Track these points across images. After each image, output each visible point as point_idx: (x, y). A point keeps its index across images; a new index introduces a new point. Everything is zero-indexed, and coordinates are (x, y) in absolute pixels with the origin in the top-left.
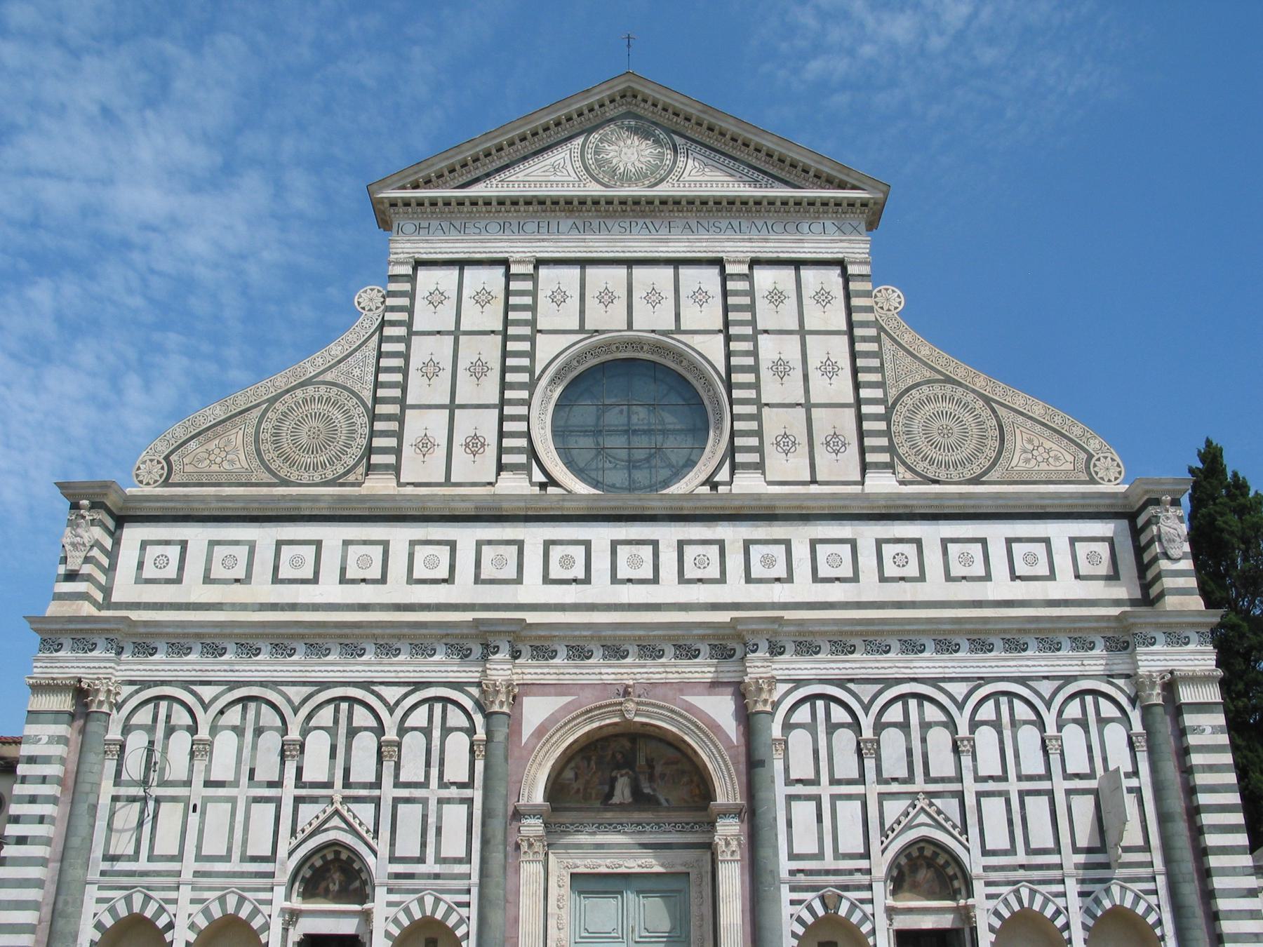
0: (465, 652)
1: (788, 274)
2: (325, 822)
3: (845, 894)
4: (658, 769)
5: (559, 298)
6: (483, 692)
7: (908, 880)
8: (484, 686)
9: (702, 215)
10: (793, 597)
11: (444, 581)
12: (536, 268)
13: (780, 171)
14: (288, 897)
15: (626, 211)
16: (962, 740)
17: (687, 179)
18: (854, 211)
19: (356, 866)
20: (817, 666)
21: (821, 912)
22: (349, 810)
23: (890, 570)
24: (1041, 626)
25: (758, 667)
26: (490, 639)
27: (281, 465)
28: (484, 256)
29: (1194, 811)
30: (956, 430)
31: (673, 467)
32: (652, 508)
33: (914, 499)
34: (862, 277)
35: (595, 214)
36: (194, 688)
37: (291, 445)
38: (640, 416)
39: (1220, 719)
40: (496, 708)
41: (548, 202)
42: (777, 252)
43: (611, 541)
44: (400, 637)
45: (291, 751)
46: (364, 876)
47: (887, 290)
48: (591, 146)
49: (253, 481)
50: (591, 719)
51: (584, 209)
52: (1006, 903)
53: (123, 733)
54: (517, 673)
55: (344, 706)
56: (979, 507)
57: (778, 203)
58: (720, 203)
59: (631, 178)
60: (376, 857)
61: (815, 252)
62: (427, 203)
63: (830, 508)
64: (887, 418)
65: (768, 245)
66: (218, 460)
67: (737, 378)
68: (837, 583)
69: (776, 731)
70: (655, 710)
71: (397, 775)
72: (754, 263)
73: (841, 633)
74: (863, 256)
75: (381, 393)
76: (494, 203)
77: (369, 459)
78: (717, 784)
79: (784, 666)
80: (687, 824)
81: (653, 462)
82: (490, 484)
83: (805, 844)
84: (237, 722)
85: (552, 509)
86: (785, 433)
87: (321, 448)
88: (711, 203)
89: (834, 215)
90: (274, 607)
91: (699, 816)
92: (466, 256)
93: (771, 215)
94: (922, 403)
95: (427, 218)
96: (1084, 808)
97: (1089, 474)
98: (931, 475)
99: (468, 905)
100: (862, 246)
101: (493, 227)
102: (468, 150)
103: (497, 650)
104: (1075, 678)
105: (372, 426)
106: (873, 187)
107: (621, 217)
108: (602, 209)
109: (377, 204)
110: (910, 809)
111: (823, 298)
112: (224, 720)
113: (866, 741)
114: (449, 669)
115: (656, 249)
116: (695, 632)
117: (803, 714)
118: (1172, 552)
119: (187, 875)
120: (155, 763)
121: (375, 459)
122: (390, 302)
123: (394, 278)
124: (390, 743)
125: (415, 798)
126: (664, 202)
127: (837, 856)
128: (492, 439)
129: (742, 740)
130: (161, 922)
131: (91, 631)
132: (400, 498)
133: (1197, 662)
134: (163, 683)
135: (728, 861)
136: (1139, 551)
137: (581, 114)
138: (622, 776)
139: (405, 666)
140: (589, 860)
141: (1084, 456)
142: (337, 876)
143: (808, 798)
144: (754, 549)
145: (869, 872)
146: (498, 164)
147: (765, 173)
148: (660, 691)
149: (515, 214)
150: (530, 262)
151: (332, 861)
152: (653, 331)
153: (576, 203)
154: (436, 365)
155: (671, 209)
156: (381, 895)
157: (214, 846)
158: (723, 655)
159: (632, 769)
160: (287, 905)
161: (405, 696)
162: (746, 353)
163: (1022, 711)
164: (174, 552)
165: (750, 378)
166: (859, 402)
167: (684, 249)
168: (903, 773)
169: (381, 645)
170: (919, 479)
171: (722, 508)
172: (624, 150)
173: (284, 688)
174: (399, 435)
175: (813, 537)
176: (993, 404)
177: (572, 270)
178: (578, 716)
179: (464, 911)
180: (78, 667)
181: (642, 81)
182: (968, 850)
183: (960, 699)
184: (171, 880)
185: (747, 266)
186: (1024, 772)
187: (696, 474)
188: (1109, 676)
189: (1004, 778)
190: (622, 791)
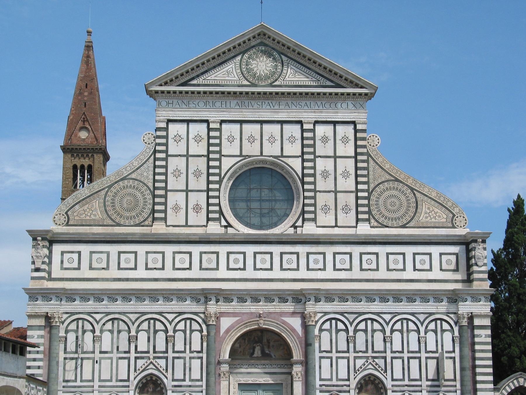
0: (198, 300)
1: (331, 127)
2: (147, 366)
5: (231, 139)
6: (205, 316)
7: (364, 389)
8: (206, 314)
11: (188, 269)
12: (221, 124)
13: (329, 76)
15: (260, 97)
16: (387, 337)
17: (288, 79)
18: (361, 97)
19: (159, 382)
20: (333, 307)
22: (156, 362)
23: (365, 266)
24: (422, 293)
25: (310, 307)
26: (208, 295)
27: (116, 217)
28: (198, 118)
29: (474, 367)
31: (279, 216)
32: (270, 239)
35: (246, 98)
36: (92, 315)
38: (265, 193)
39: (489, 332)
40: (211, 323)
42: (326, 118)
43: (254, 252)
44: (172, 294)
45: (132, 339)
46: (162, 386)
49: (105, 224)
50: (247, 327)
53: (65, 333)
54: (218, 308)
55: (152, 321)
56: (403, 239)
57: (328, 94)
60: (167, 379)
63: (342, 239)
64: (368, 198)
65: (322, 114)
66: (89, 214)
68: (343, 271)
69: (316, 332)
70: (271, 323)
71: (173, 348)
73: (343, 294)
78: (293, 352)
79: (320, 307)
80: (282, 365)
81: (271, 214)
83: (326, 375)
84: (110, 328)
85: (230, 238)
89: (352, 99)
90: (119, 280)
91: (287, 362)
94: (384, 191)
95: (170, 99)
96: (432, 364)
97: (453, 224)
98: (385, 224)
100: (364, 115)
103: (210, 300)
104: (434, 314)
107: (258, 100)
110: (366, 363)
111: (345, 140)
112: (105, 328)
113: (350, 337)
114: (192, 307)
115: (273, 116)
116: (287, 293)
117: (327, 326)
118: (479, 263)
119: (96, 387)
120: (80, 345)
121: (157, 215)
122: (158, 141)
124: (171, 336)
125: (181, 357)
127: (338, 380)
129: (304, 335)
131: (49, 293)
133: (482, 309)
134: (80, 313)
135: (297, 381)
136: (469, 259)
138: (257, 346)
139: (175, 306)
140: (245, 378)
141: (451, 215)
142: (151, 386)
143: (327, 358)
144: (311, 256)
145: (349, 386)
146: (202, 70)
147: (323, 76)
148: (273, 315)
149: (211, 98)
151: (149, 380)
152: (271, 156)
154: (179, 171)
155: (280, 96)
157: (106, 375)
158: (297, 301)
159: (261, 343)
161: (176, 317)
163: (412, 326)
164: (75, 256)
165: (311, 179)
166: (357, 191)
167: (285, 116)
168: (364, 349)
169: (165, 297)
170: (380, 225)
171: (299, 239)
172: (260, 63)
173: (128, 315)
174: (165, 204)
177: (236, 126)
178: (242, 325)
180: (46, 308)
182: (387, 379)
183: (387, 321)
184: (90, 389)
185: (313, 125)
186: (410, 350)
188: (447, 313)
189: (402, 352)
190: (258, 352)
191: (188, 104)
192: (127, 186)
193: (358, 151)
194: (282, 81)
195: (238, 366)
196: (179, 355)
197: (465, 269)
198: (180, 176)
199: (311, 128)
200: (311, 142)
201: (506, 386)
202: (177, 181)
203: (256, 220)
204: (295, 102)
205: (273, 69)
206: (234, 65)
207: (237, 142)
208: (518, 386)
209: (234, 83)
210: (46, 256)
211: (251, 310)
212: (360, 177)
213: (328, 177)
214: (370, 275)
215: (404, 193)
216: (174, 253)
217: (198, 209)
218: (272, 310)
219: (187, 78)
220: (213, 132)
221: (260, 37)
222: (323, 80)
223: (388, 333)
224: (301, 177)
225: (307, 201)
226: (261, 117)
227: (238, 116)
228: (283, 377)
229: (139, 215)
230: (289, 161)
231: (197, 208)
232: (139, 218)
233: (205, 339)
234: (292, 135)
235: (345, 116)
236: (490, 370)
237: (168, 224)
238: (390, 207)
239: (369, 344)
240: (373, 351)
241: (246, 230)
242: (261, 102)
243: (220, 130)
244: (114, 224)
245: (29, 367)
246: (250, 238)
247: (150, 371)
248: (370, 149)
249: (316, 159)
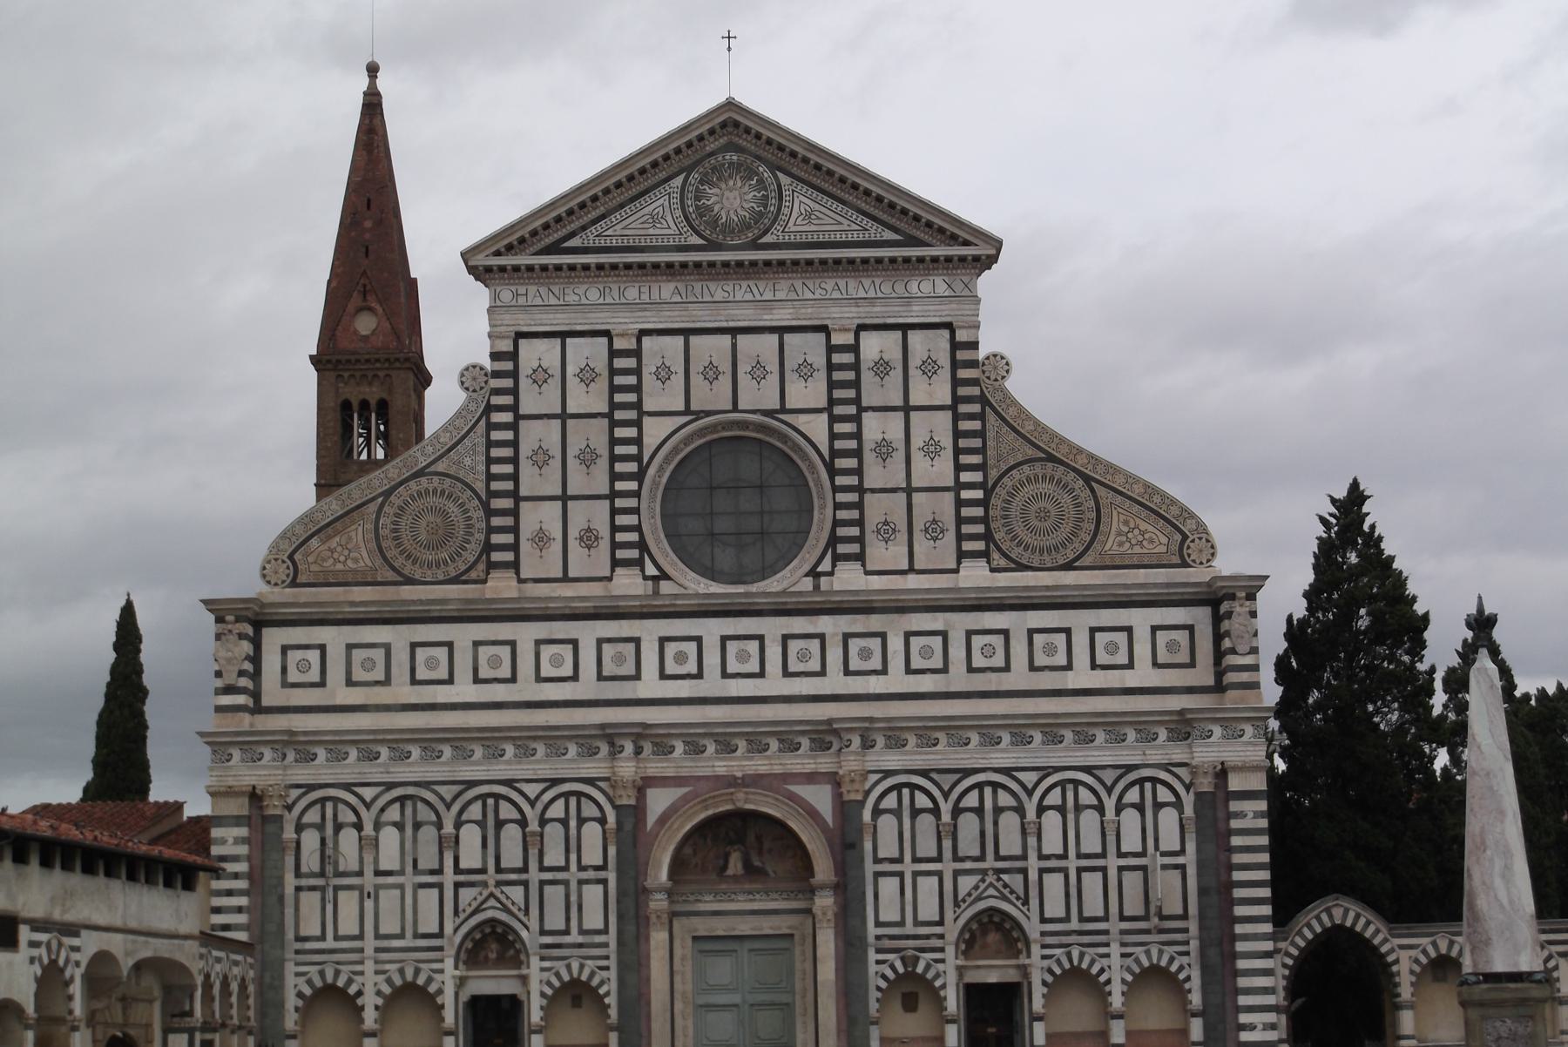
2: (482, 903)
3: (922, 955)
4: (767, 845)
5: (663, 374)
10: (887, 689)
12: (639, 341)
14: (456, 968)
16: (1029, 823)
19: (510, 938)
21: (901, 970)
22: (502, 892)
23: (978, 661)
30: (1053, 513)
35: (697, 277)
37: (411, 542)
39: (1263, 805)
40: (625, 801)
44: (535, 738)
46: (518, 946)
48: (691, 189)
49: (379, 579)
50: (706, 808)
51: (686, 272)
52: (1059, 962)
53: (296, 833)
61: (923, 316)
66: (342, 558)
69: (867, 815)
71: (541, 861)
72: (862, 328)
83: (889, 913)
87: (439, 545)
89: (945, 272)
94: (1022, 484)
96: (1133, 881)
97: (1182, 556)
99: (607, 968)
105: (488, 521)
106: (983, 241)
110: (981, 884)
112: (386, 817)
113: (944, 825)
117: (890, 801)
118: (1239, 649)
119: (369, 951)
120: (329, 857)
121: (496, 556)
124: (533, 834)
127: (917, 923)
128: (605, 531)
130: (352, 990)
136: (1218, 637)
138: (735, 851)
141: (1178, 537)
142: (494, 946)
146: (594, 214)
147: (874, 219)
151: (490, 934)
152: (759, 410)
154: (546, 452)
156: (535, 962)
157: (389, 925)
160: (457, 973)
163: (1086, 797)
164: (314, 656)
165: (852, 463)
166: (960, 486)
167: (789, 317)
168: (976, 852)
170: (1013, 566)
172: (727, 193)
173: (436, 787)
174: (515, 530)
175: (908, 629)
176: (1093, 484)
179: (604, 974)
182: (1028, 918)
183: (1030, 786)
189: (1065, 856)
190: (735, 865)
193: (959, 394)
195: (692, 898)
196: (554, 876)
197: (1211, 661)
198: (548, 464)
200: (850, 375)
201: (1302, 927)
202: (540, 475)
203: (725, 558)
204: (810, 283)
207: (678, 380)
208: (1330, 925)
209: (669, 242)
210: (247, 658)
211: (717, 769)
214: (990, 681)
216: (538, 643)
218: (763, 770)
219: (560, 233)
222: (874, 227)
223: (1031, 814)
224: (827, 458)
227: (678, 319)
228: (793, 920)
230: (801, 421)
231: (589, 538)
233: (611, 839)
234: (805, 360)
235: (929, 311)
236: (1266, 892)
238: (1035, 522)
239: (988, 841)
240: (998, 857)
241: (702, 585)
243: (637, 353)
244: (400, 579)
245: (217, 910)
247: (490, 914)
248: (987, 388)
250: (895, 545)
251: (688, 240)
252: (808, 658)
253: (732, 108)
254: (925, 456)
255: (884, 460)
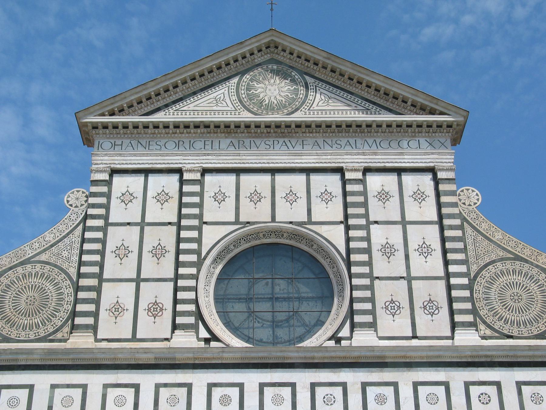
1: (393, 178)
5: (220, 197)
9: (327, 135)
12: (203, 175)
13: (385, 102)
18: (442, 130)
28: (163, 166)
30: (524, 297)
31: (307, 326)
33: (494, 350)
34: (449, 180)
35: (247, 135)
37: (12, 310)
38: (281, 287)
41: (212, 126)
47: (468, 190)
48: (244, 84)
51: (239, 131)
57: (384, 126)
58: (340, 126)
59: (274, 108)
61: (412, 162)
62: (120, 127)
63: (427, 357)
64: (470, 287)
67: (354, 257)
72: (367, 171)
74: (449, 164)
75: (84, 270)
76: (171, 127)
77: (73, 321)
81: (292, 322)
82: (167, 339)
85: (214, 358)
86: (392, 300)
87: (38, 312)
88: (334, 126)
89: (427, 134)
92: (150, 166)
93: (379, 134)
94: (497, 276)
95: (120, 138)
98: (506, 332)
101: (171, 145)
102: (153, 87)
105: (76, 295)
106: (455, 112)
107: (267, 137)
108: (253, 131)
109: (82, 127)
111: (419, 196)
115: (293, 161)
121: (78, 321)
122: (92, 200)
123: (95, 183)
126: (298, 126)
132: (97, 351)
137: (236, 61)
146: (174, 98)
147: (374, 103)
149: (187, 135)
150: (198, 171)
153: (232, 127)
154: (126, 248)
155: (304, 130)
162: (361, 239)
165: (364, 257)
166: (448, 275)
170: (497, 335)
171: (345, 358)
174: (97, 302)
177: (230, 177)
181: (282, 36)
187: (324, 331)
191: (147, 146)
192: (30, 274)
194: (306, 111)
199: (359, 178)
200: (361, 199)
202: (121, 264)
205: (292, 87)
206: (227, 90)
207: (231, 202)
212: (451, 252)
213: (394, 255)
215: (535, 279)
217: (157, 311)
219: (149, 108)
220: (188, 186)
221: (269, 51)
222: (374, 108)
224: (345, 256)
225: (357, 294)
226: (272, 163)
229: (47, 322)
232: (46, 327)
235: (417, 159)
237: (98, 337)
242: (272, 140)
246: (253, 358)
248: (464, 210)
249: (371, 226)
250: (400, 319)
251: (241, 113)
252: (332, 402)
253: (275, 33)
254: (420, 255)
255: (389, 258)
